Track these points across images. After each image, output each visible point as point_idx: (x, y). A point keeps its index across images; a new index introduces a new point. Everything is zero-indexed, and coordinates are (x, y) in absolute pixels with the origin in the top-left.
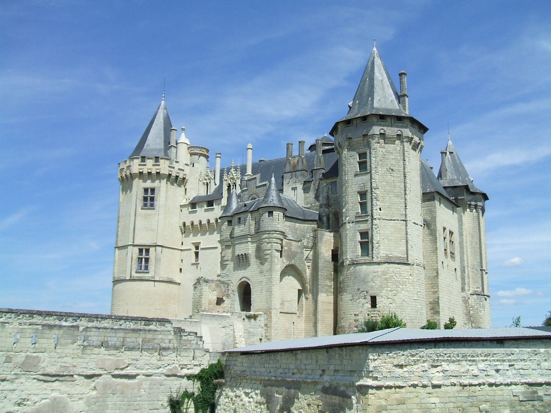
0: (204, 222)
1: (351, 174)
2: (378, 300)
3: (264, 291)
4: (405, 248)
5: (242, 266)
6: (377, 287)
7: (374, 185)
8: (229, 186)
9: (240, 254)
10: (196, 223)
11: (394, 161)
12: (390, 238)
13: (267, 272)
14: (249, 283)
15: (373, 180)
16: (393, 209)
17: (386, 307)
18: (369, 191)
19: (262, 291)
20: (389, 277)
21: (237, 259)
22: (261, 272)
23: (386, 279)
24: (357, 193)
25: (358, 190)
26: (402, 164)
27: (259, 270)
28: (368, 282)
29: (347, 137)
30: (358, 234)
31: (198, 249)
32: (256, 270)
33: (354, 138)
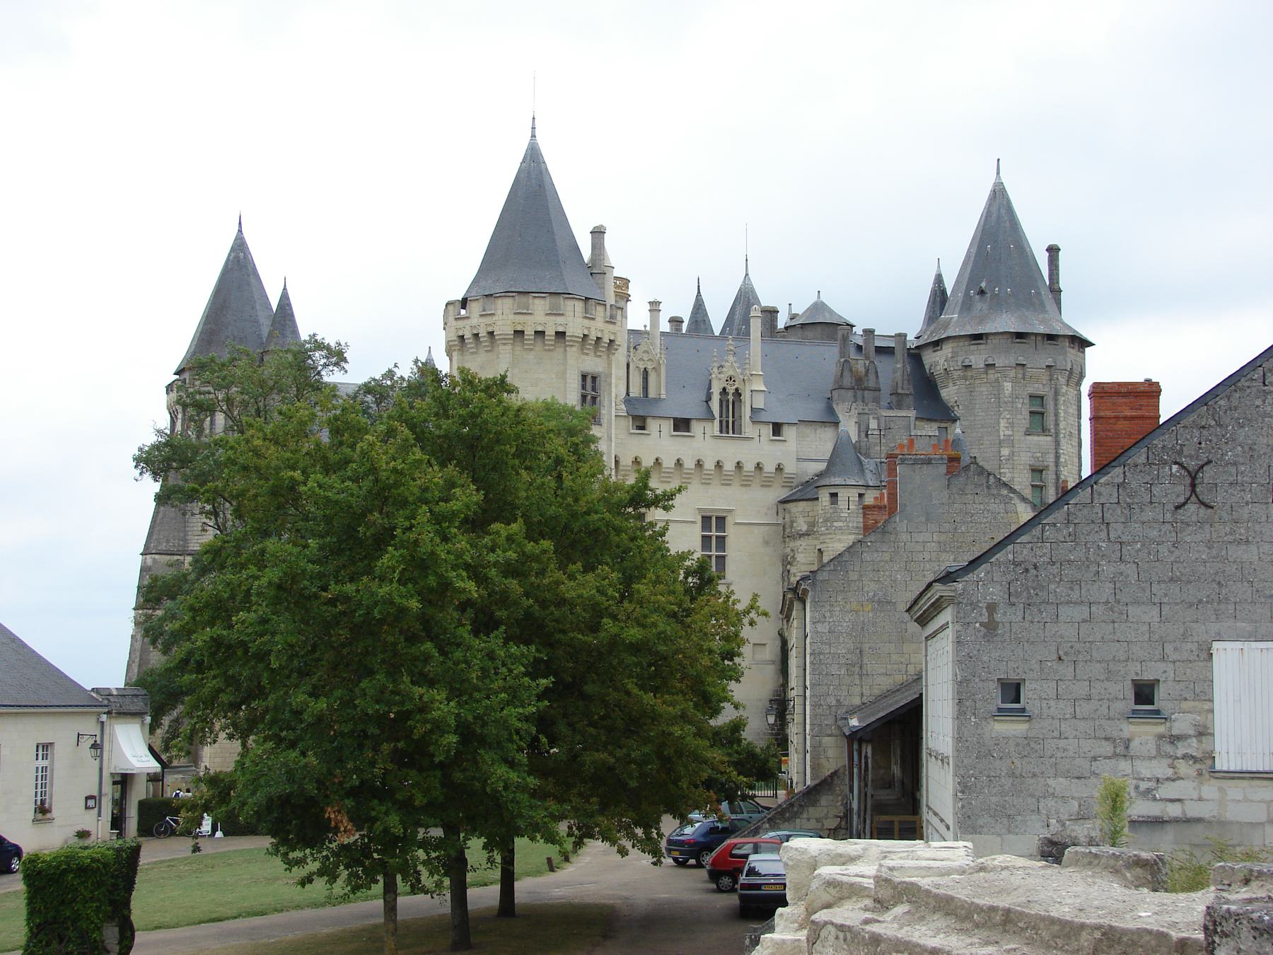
15: (1062, 451)
18: (1052, 468)
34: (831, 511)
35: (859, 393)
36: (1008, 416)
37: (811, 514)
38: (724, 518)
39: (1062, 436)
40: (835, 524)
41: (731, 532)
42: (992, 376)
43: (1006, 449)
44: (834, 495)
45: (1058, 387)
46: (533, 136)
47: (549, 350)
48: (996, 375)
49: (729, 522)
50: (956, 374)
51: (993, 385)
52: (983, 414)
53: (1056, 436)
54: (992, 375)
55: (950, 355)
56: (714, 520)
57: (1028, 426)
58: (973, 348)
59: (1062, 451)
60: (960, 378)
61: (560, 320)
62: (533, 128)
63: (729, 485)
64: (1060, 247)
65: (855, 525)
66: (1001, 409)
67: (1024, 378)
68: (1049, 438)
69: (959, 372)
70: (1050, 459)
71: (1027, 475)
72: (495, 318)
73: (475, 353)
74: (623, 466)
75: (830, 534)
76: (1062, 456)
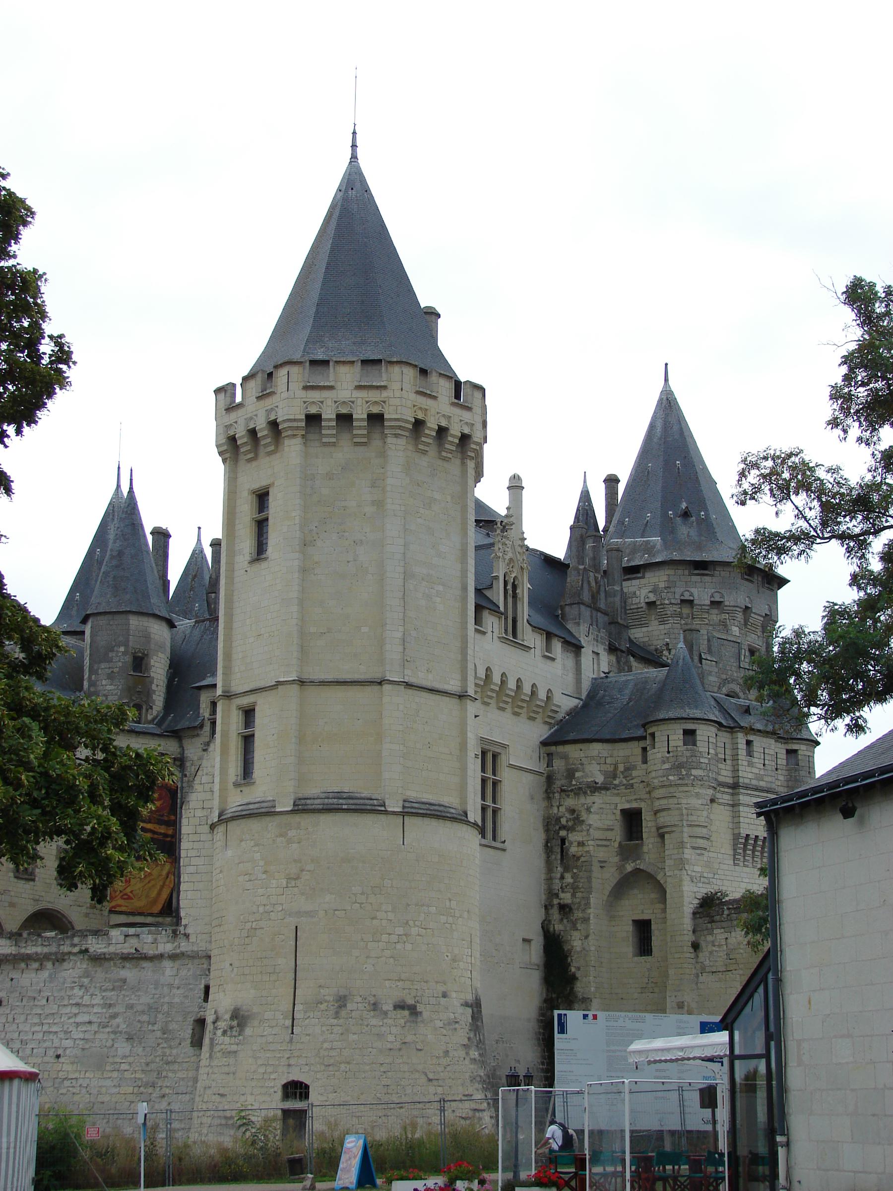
33: (755, 614)
34: (688, 754)
35: (594, 613)
37: (609, 761)
40: (694, 772)
42: (714, 617)
44: (690, 734)
46: (354, 157)
47: (445, 459)
48: (724, 616)
49: (503, 760)
50: (670, 610)
55: (662, 585)
60: (675, 615)
61: (466, 416)
62: (354, 146)
72: (385, 394)
73: (334, 444)
75: (686, 785)
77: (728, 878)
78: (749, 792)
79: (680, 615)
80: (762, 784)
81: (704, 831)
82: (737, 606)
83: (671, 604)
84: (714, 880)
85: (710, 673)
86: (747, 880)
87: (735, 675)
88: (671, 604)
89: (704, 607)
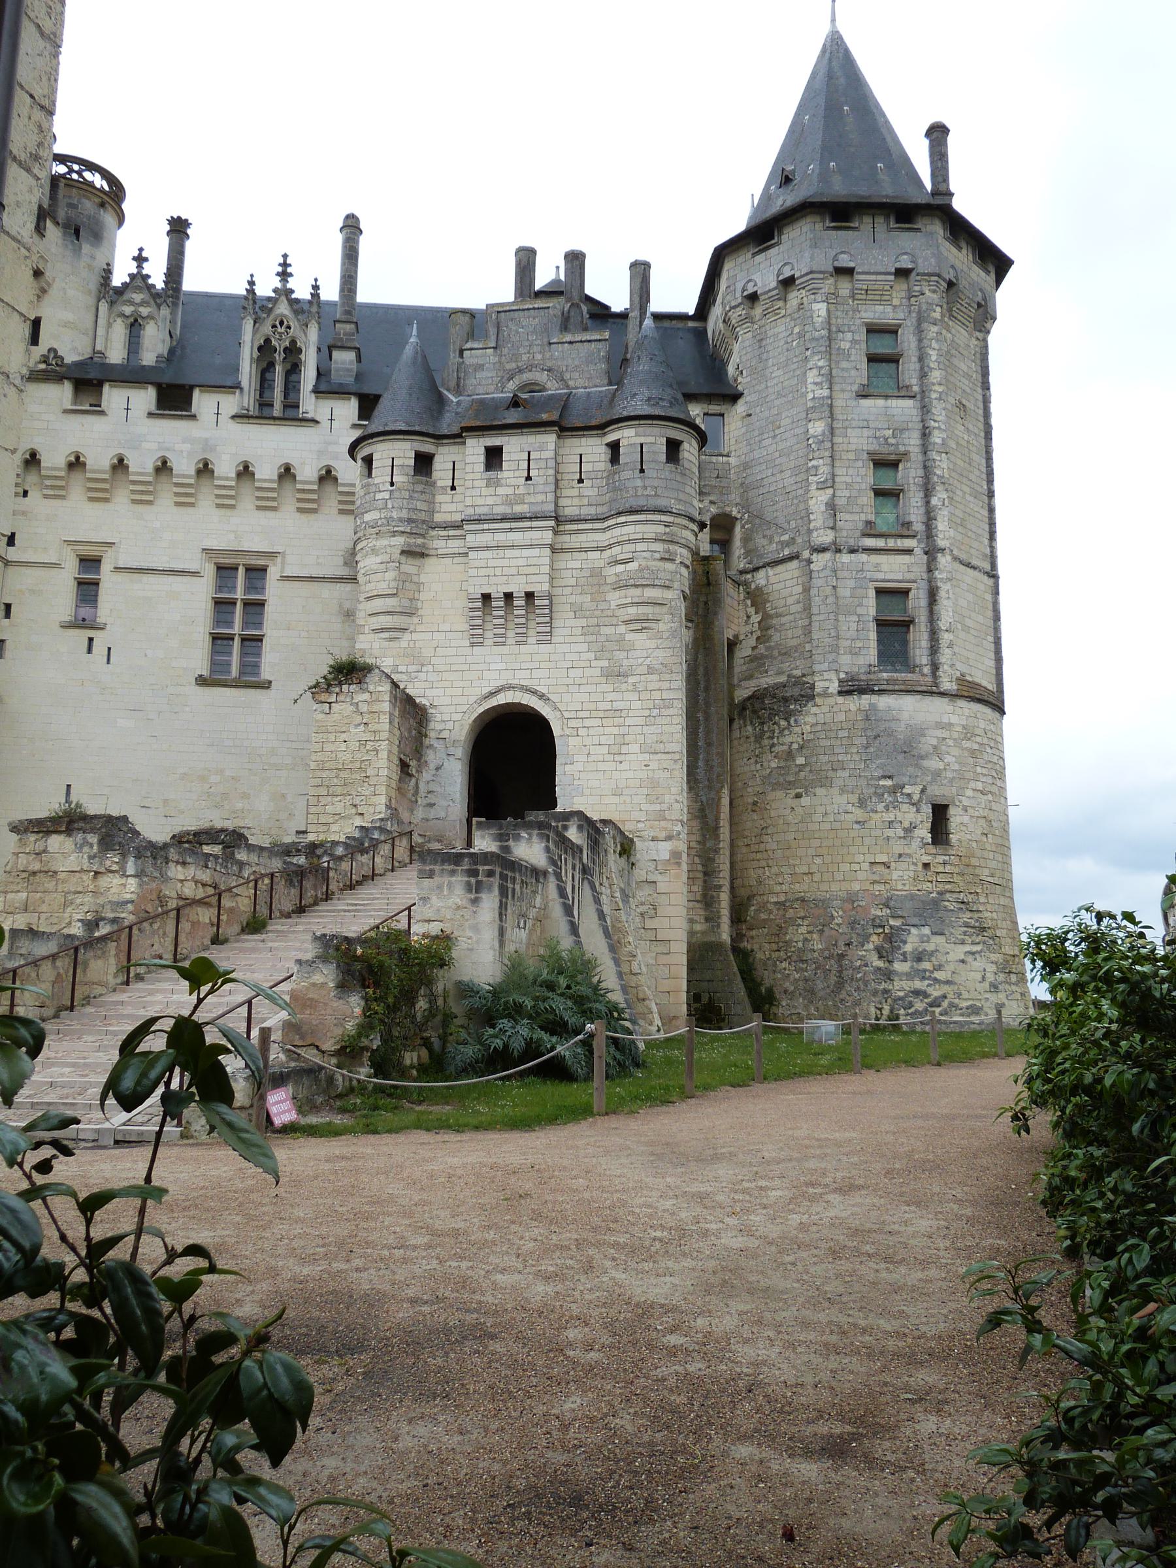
0: (141, 463)
1: (843, 391)
2: (956, 819)
3: (635, 748)
4: (992, 663)
5: (496, 644)
6: (949, 775)
7: (937, 438)
8: (265, 348)
9: (497, 591)
10: (99, 460)
11: (967, 382)
12: (969, 622)
13: (655, 677)
14: (545, 710)
15: (933, 424)
16: (970, 534)
17: (974, 844)
19: (624, 749)
20: (976, 747)
21: (472, 609)
22: (616, 674)
23: (973, 753)
24: (865, 456)
25: (871, 448)
26: (980, 398)
27: (605, 663)
28: (922, 757)
29: (837, 264)
30: (872, 593)
31: (98, 571)
32: (582, 664)
36: (821, 364)
38: (263, 570)
39: (934, 396)
41: (274, 591)
43: (818, 424)
45: (924, 307)
49: (273, 573)
51: (796, 315)
52: (780, 372)
53: (923, 398)
54: (794, 297)
56: (241, 571)
57: (865, 382)
58: (760, 258)
59: (933, 424)
63: (274, 509)
64: (948, 125)
65: (404, 514)
66: (808, 353)
67: (853, 297)
68: (909, 403)
69: (739, 311)
70: (912, 442)
71: (863, 471)
74: (47, 468)
76: (936, 433)
77: (454, 668)
78: (486, 526)
79: (748, 319)
80: (518, 509)
81: (391, 603)
82: (811, 272)
83: (732, 308)
84: (422, 676)
85: (481, 367)
86: (503, 666)
87: (539, 357)
88: (732, 308)
89: (771, 294)
